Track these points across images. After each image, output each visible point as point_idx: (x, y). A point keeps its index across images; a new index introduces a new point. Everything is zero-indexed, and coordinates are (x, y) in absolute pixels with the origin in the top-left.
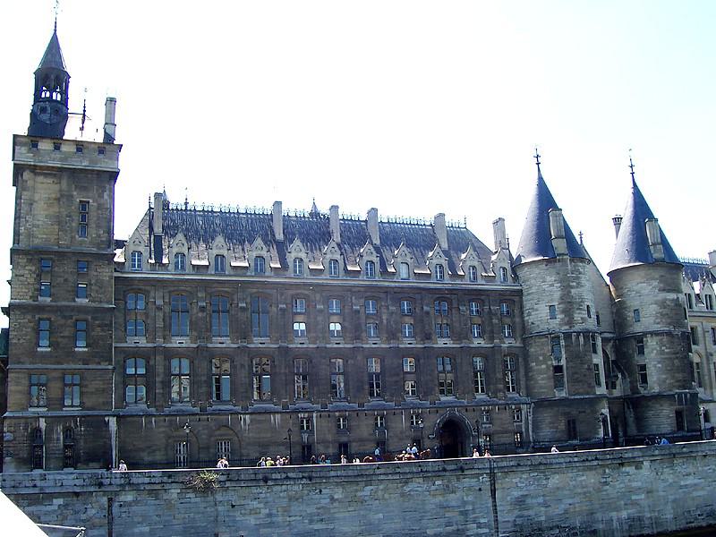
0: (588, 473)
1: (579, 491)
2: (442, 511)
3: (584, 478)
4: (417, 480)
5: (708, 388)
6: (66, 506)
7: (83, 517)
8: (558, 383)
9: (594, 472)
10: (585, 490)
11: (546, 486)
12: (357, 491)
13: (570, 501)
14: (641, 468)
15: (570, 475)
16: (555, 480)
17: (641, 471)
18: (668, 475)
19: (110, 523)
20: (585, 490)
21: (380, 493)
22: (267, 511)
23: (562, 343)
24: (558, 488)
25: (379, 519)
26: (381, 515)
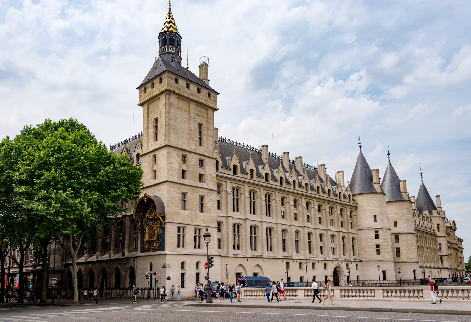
8: (378, 252)
23: (380, 233)
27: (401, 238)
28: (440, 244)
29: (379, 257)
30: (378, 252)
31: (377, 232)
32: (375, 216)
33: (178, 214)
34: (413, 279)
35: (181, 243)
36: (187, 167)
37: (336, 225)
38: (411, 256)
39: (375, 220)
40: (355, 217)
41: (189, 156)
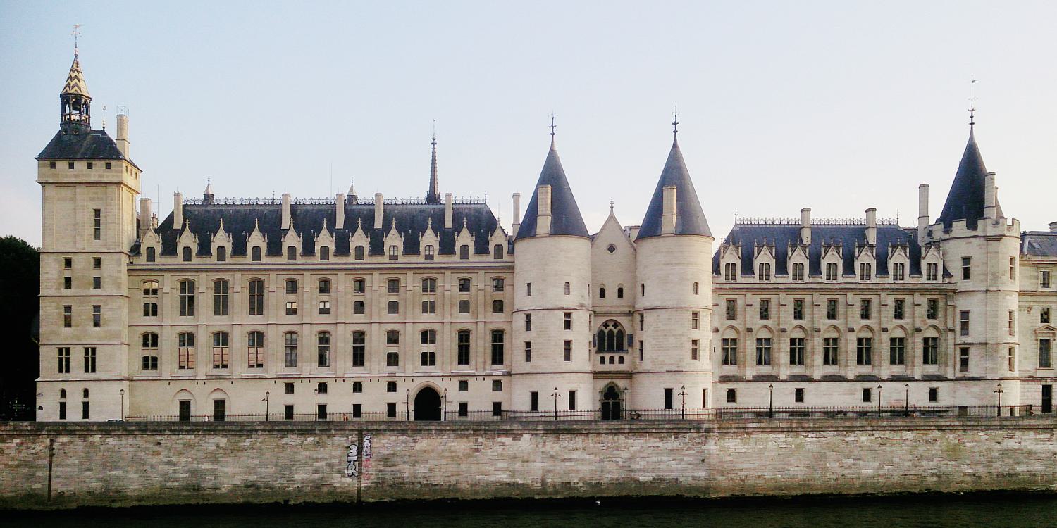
0: (459, 440)
1: (447, 454)
2: (310, 462)
3: (453, 444)
4: (292, 436)
5: (742, 366)
6: (21, 444)
7: (33, 451)
8: (528, 358)
9: (465, 440)
10: (453, 454)
11: (412, 448)
12: (239, 441)
13: (436, 463)
14: (520, 440)
15: (440, 441)
16: (423, 443)
17: (520, 442)
18: (552, 446)
19: (52, 455)
20: (453, 454)
21: (258, 445)
22: (166, 453)
24: (425, 451)
25: (256, 465)
26: (257, 462)
27: (649, 318)
28: (965, 314)
29: (527, 367)
30: (528, 358)
31: (529, 316)
32: (529, 285)
33: (57, 334)
34: (663, 407)
35: (64, 366)
36: (72, 272)
37: (438, 310)
38: (661, 359)
39: (529, 294)
40: (507, 289)
41: (74, 258)
